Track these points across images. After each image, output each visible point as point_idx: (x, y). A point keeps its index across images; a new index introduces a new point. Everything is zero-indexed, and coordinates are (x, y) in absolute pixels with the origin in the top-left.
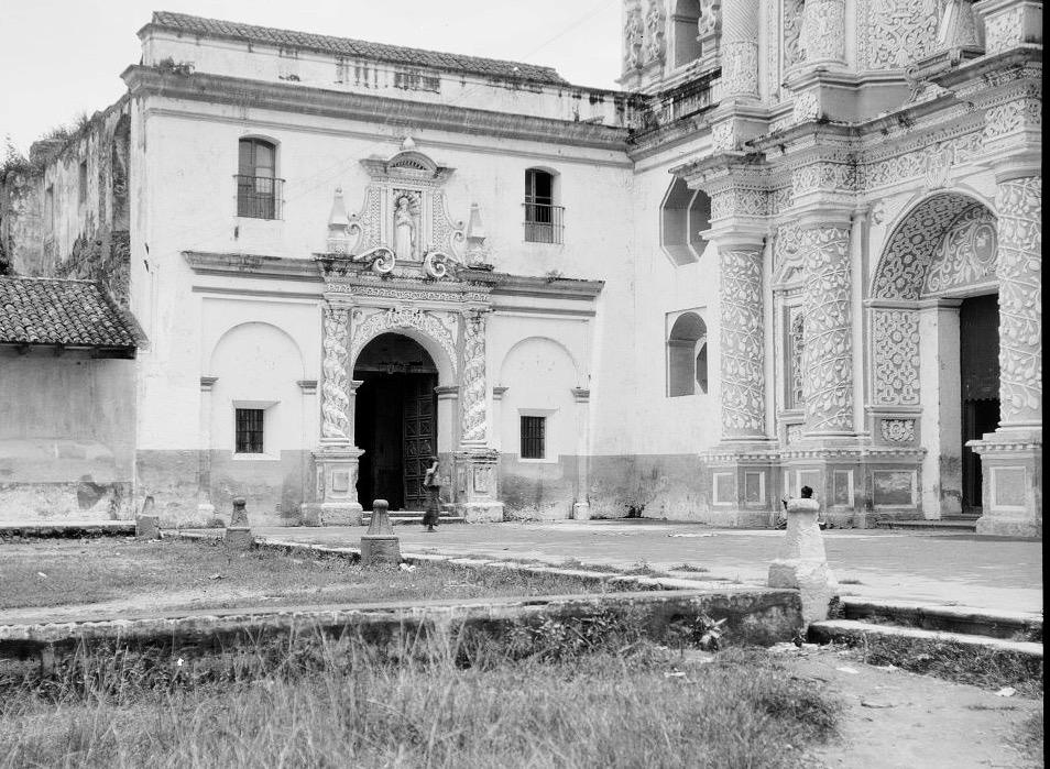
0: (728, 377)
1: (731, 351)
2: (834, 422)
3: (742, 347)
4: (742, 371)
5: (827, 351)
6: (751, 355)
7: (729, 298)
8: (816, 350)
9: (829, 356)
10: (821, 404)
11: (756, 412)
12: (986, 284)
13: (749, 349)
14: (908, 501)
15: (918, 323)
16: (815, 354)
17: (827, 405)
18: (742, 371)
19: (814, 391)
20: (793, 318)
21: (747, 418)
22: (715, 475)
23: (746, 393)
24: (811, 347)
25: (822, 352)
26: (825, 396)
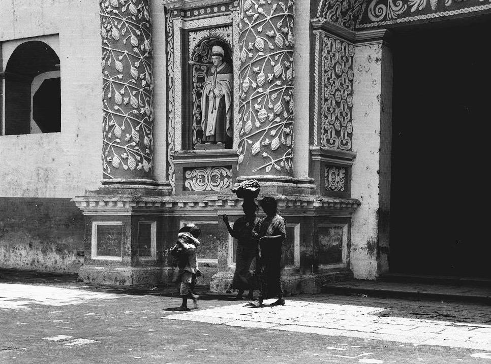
0: (116, 107)
1: (120, 76)
2: (282, 164)
3: (134, 72)
4: (134, 101)
5: (277, 75)
6: (144, 83)
7: (115, 11)
8: (262, 74)
9: (278, 82)
10: (267, 141)
11: (148, 151)
12: (460, 11)
13: (142, 76)
14: (339, 260)
15: (352, 57)
16: (261, 78)
17: (275, 143)
18: (134, 101)
19: (258, 124)
20: (193, 44)
21: (138, 158)
22: (95, 225)
23: (138, 128)
24: (256, 69)
25: (270, 77)
26: (273, 132)
